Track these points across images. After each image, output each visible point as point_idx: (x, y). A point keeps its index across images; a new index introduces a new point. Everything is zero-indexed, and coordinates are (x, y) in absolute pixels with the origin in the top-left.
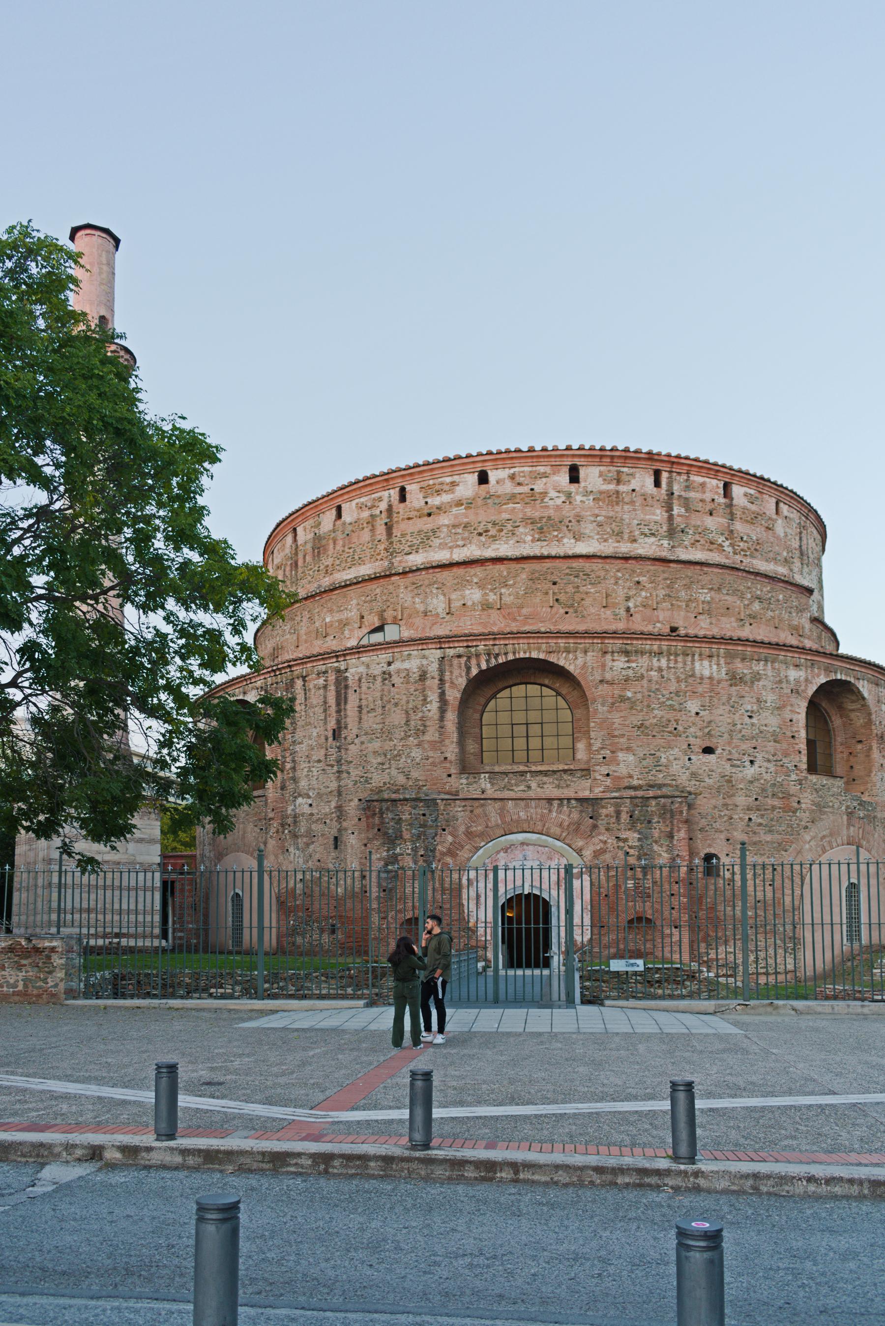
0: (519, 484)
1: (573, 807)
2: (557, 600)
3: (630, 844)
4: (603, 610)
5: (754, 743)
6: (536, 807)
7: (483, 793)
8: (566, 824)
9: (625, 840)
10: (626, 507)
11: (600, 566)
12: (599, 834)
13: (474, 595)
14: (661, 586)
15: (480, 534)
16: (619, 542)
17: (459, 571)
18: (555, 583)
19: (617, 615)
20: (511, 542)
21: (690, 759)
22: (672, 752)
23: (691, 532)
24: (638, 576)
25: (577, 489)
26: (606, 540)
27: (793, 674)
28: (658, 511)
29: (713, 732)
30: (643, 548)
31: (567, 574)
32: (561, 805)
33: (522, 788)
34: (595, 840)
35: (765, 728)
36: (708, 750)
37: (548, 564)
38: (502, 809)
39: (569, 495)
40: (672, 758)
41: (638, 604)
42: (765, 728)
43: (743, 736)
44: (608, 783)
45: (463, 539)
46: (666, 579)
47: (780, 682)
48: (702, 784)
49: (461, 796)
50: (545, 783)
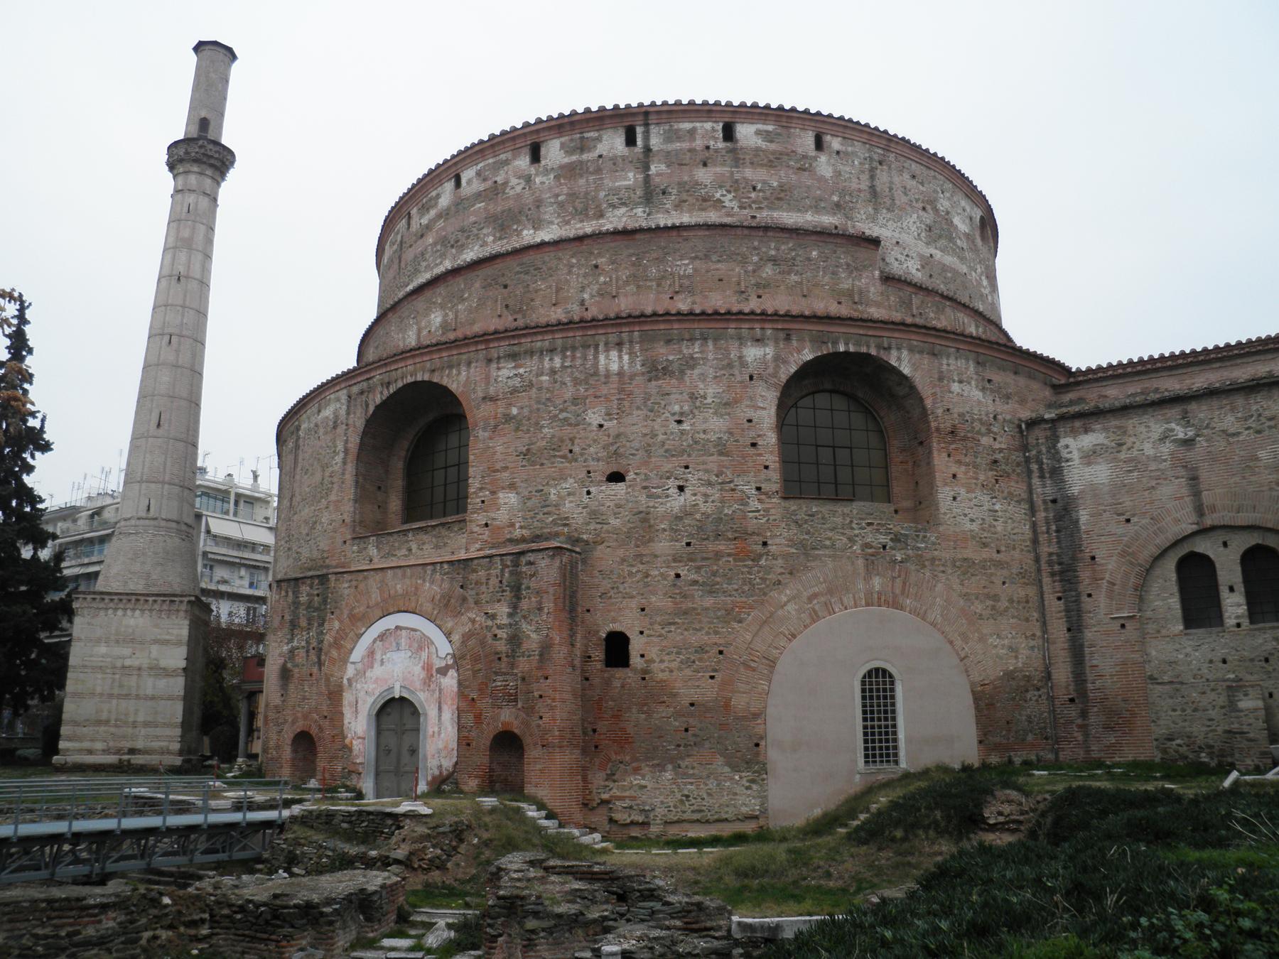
0: (485, 180)
1: (445, 574)
2: (507, 306)
3: (498, 622)
4: (553, 309)
5: (684, 459)
6: (411, 576)
7: (371, 561)
8: (438, 597)
9: (493, 617)
10: (591, 178)
11: (552, 254)
12: (468, 609)
13: (436, 318)
14: (623, 266)
15: (452, 246)
16: (582, 221)
17: (428, 293)
18: (505, 287)
19: (569, 312)
20: (476, 248)
21: (589, 493)
22: (564, 485)
23: (675, 191)
24: (596, 258)
25: (537, 171)
26: (568, 223)
27: (753, 353)
28: (631, 175)
29: (622, 450)
30: (611, 222)
31: (519, 273)
32: (434, 571)
33: (404, 552)
34: (464, 618)
35: (702, 436)
36: (616, 477)
37: (499, 265)
38: (382, 581)
39: (528, 179)
40: (564, 492)
41: (594, 293)
42: (702, 436)
43: (666, 451)
44: (485, 537)
45: (441, 256)
46: (631, 255)
47: (730, 365)
48: (605, 527)
49: (352, 569)
50: (424, 544)
